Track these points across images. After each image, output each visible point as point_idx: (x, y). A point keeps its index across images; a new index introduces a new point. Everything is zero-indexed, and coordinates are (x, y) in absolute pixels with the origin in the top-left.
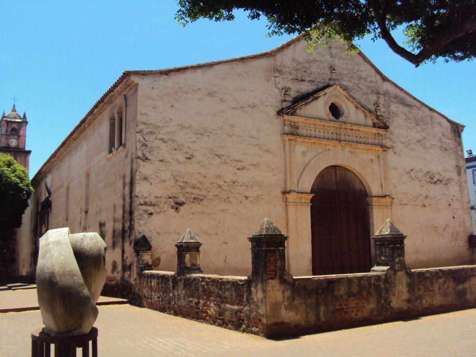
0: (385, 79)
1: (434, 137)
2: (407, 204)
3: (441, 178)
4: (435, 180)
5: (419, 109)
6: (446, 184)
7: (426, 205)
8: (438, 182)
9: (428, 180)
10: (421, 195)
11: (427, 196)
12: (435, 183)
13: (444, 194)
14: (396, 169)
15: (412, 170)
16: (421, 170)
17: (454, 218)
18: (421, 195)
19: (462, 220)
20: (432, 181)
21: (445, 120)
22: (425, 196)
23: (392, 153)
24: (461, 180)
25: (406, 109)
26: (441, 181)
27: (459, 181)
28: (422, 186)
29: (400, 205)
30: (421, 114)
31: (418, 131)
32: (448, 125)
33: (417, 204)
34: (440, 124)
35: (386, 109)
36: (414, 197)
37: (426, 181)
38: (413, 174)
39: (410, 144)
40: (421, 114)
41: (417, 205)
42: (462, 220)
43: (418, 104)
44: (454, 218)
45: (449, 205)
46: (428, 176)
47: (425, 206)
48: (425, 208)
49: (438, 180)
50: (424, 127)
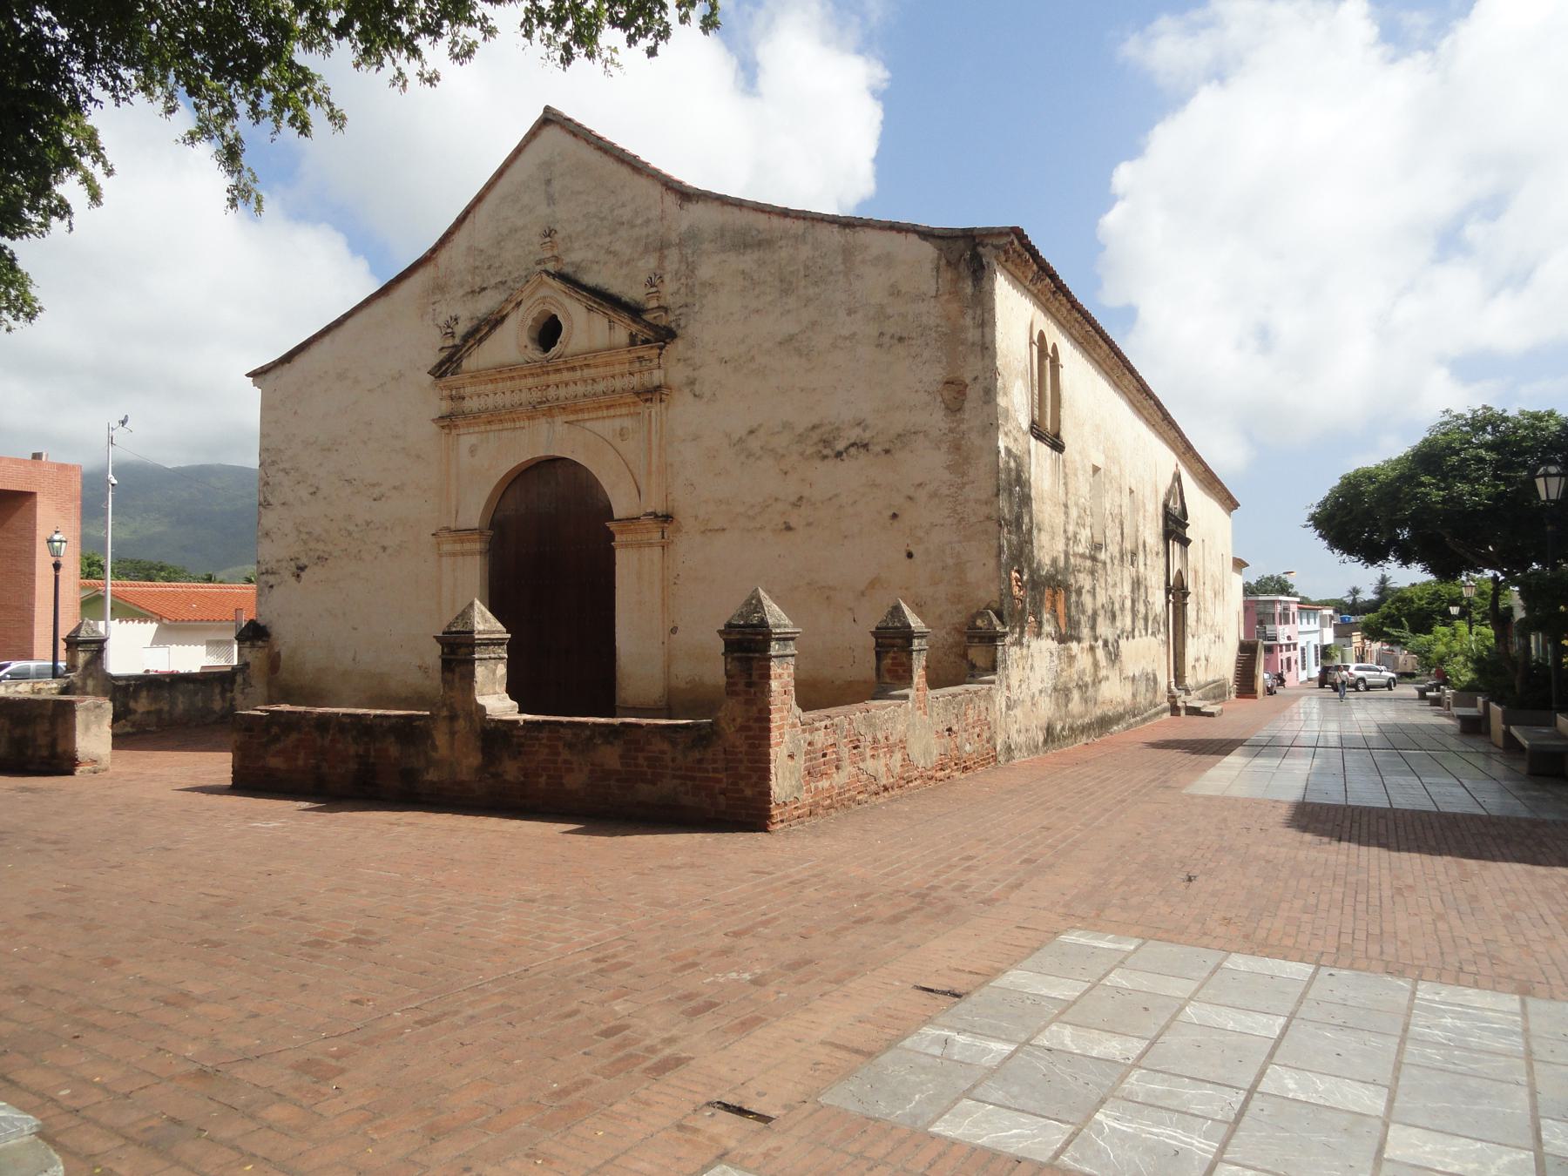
0: (686, 195)
1: (850, 312)
2: (724, 530)
3: (867, 436)
4: (840, 446)
5: (799, 239)
6: (887, 451)
7: (792, 525)
8: (853, 451)
9: (809, 451)
10: (776, 499)
11: (801, 498)
12: (839, 455)
13: (874, 485)
14: (696, 438)
15: (751, 432)
16: (787, 426)
17: (910, 555)
18: (776, 499)
19: (950, 562)
20: (826, 452)
21: (913, 238)
22: (793, 498)
23: (690, 398)
24: (964, 427)
25: (748, 261)
26: (865, 446)
27: (951, 430)
28: (786, 473)
29: (703, 532)
30: (805, 252)
31: (789, 311)
32: (928, 250)
33: (759, 526)
34: (887, 260)
35: (684, 280)
36: (753, 506)
37: (802, 454)
38: (754, 444)
40: (805, 252)
41: (762, 528)
42: (950, 562)
43: (799, 226)
44: (910, 555)
45: (895, 516)
46: (815, 436)
47: (789, 528)
48: (790, 534)
49: (853, 445)
50: (811, 291)
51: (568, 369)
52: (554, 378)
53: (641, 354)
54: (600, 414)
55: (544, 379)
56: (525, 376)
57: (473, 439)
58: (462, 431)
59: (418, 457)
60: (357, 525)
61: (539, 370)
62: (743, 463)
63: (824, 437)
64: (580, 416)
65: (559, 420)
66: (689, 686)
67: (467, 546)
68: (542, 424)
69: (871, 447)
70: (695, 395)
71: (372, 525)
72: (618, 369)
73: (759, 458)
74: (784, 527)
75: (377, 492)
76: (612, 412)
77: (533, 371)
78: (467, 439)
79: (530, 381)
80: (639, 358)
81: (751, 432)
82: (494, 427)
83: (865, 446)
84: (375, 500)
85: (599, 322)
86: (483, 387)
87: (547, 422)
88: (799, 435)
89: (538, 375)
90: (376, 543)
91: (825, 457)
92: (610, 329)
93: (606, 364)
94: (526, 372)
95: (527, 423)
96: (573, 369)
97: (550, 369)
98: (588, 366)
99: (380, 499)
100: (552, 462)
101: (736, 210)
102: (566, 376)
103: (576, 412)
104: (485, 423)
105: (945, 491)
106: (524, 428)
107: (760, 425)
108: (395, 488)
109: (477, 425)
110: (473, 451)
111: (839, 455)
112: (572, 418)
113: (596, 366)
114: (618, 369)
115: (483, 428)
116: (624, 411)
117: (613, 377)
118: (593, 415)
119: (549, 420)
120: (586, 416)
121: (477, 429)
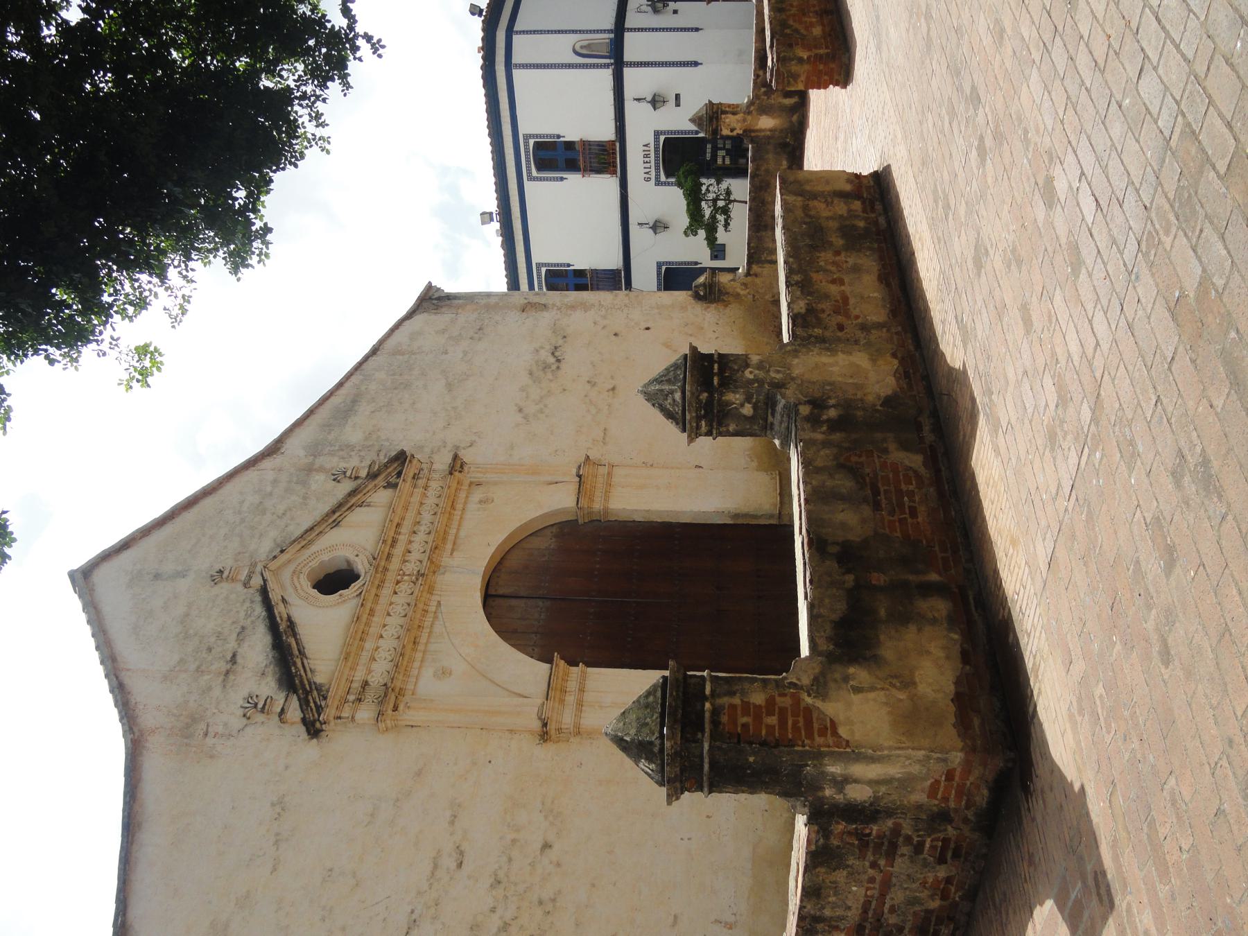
2: (605, 429)
4: (552, 360)
7: (612, 386)
9: (550, 376)
11: (588, 382)
12: (558, 361)
14: (512, 447)
16: (522, 389)
17: (648, 329)
20: (554, 367)
22: (588, 387)
24: (558, 304)
26: (556, 348)
27: (559, 309)
28: (564, 390)
29: (604, 443)
37: (551, 381)
39: (455, 408)
44: (648, 329)
47: (613, 389)
49: (553, 354)
51: (392, 546)
52: (395, 564)
53: (411, 475)
54: (457, 518)
55: (391, 577)
56: (376, 595)
57: (428, 673)
58: (410, 686)
59: (419, 773)
60: (493, 910)
61: (378, 575)
62: (547, 416)
63: (541, 368)
64: (451, 538)
65: (446, 560)
66: (756, 460)
67: (572, 685)
68: (444, 580)
69: (558, 345)
70: (470, 446)
71: (501, 874)
72: (416, 499)
73: (546, 406)
74: (611, 393)
75: (449, 862)
76: (459, 506)
77: (377, 582)
78: (426, 683)
79: (386, 591)
80: (414, 478)
81: (520, 410)
82: (423, 640)
83: (556, 348)
84: (460, 865)
85: (358, 516)
86: (364, 653)
87: (444, 574)
88: (534, 382)
89: (383, 581)
90: (532, 865)
91: (558, 368)
92: (368, 506)
93: (406, 508)
94: (374, 591)
95: (435, 598)
96: (394, 541)
97: (383, 563)
98: (398, 525)
99: (462, 853)
100: (489, 598)
101: (312, 417)
102: (398, 550)
103: (444, 539)
104: (414, 650)
105: (603, 312)
106: (439, 602)
107: (516, 405)
108: (452, 823)
109: (411, 660)
110: (444, 673)
111: (558, 361)
112: (449, 546)
113: (403, 519)
114: (416, 499)
115: (419, 655)
116: (462, 495)
117: (421, 504)
118: (455, 524)
119: (442, 570)
120: (453, 531)
121: (417, 664)
